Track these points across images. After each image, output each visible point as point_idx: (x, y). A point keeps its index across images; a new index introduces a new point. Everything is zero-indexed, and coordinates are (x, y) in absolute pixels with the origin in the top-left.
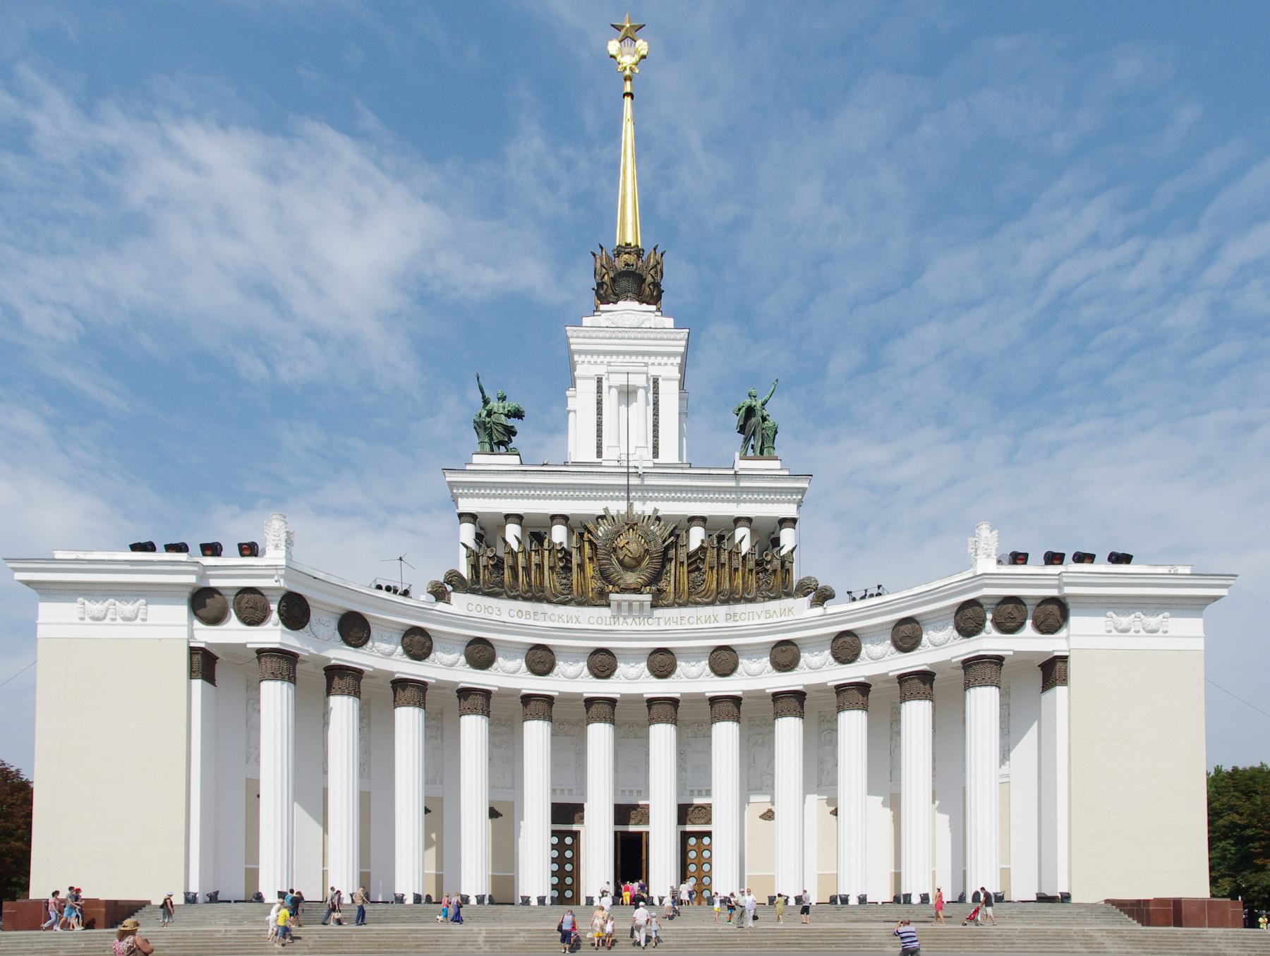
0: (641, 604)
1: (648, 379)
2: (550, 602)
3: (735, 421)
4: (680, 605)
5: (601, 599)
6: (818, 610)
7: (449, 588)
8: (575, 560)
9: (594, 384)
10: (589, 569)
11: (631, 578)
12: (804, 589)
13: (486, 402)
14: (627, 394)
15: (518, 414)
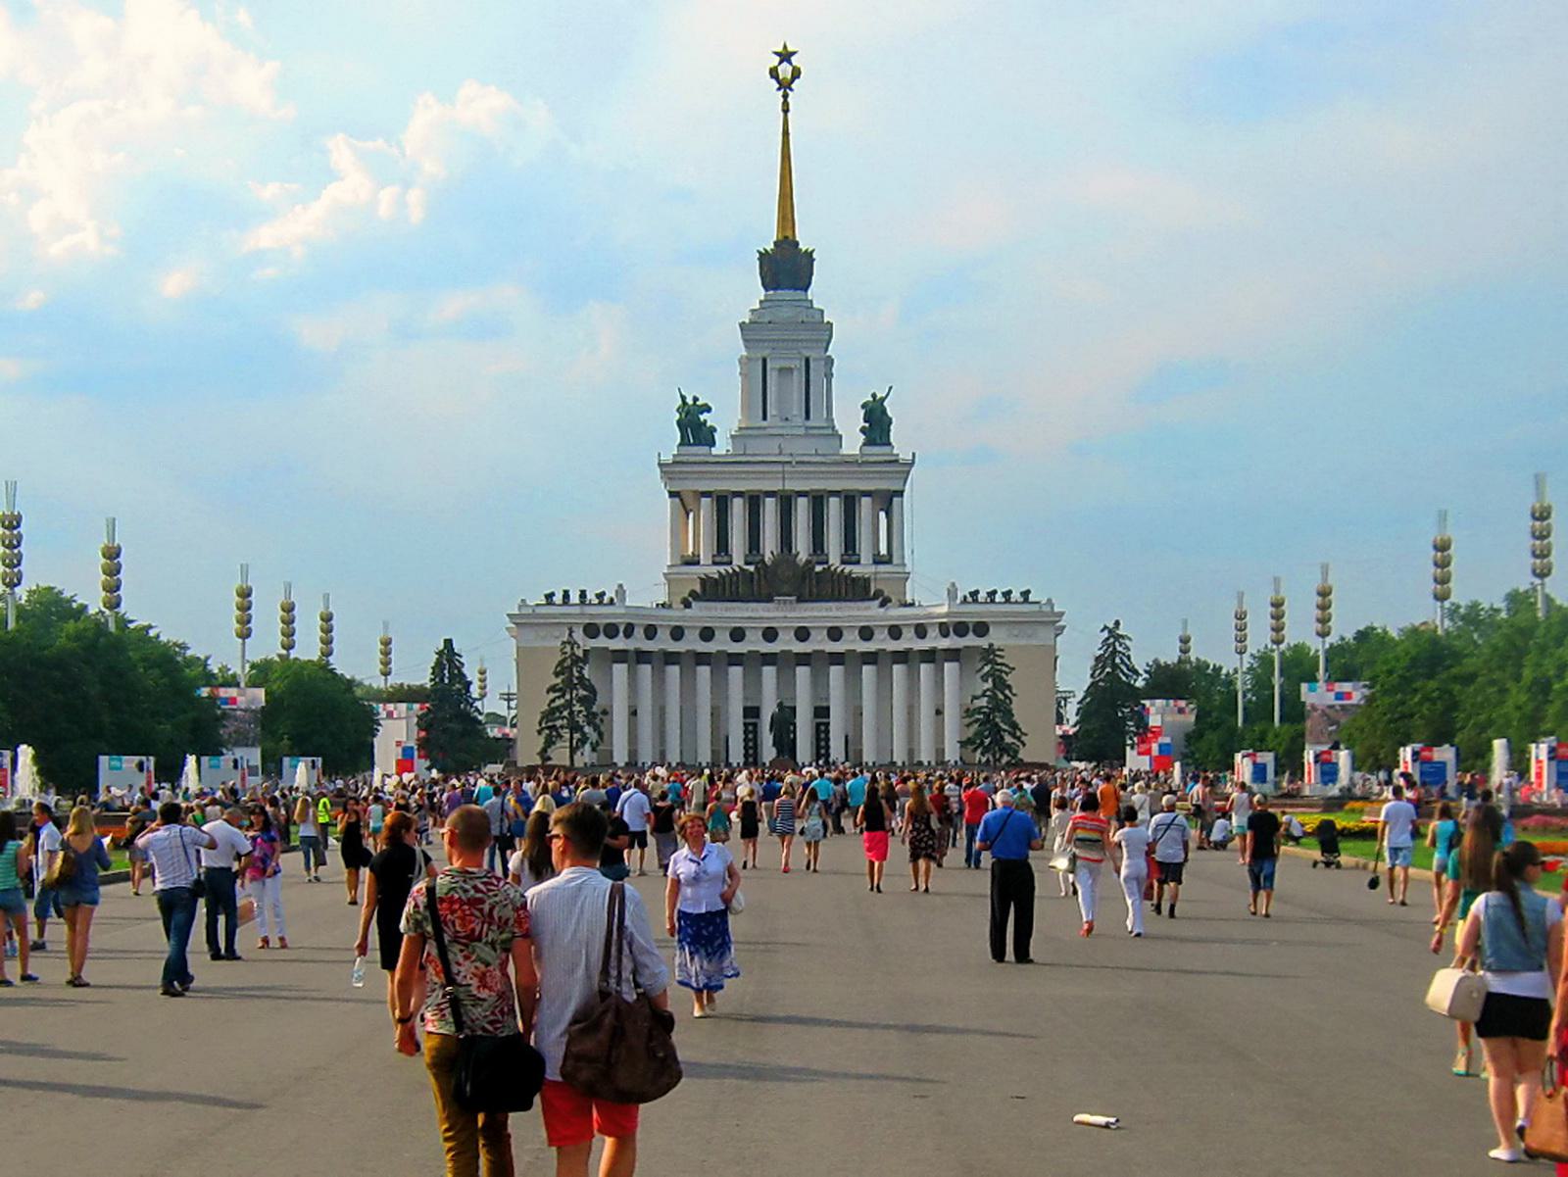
0: (791, 602)
1: (801, 360)
2: (742, 601)
3: (862, 412)
4: (812, 601)
5: (770, 600)
6: (882, 610)
7: (690, 599)
8: (756, 576)
9: (760, 363)
10: (763, 582)
11: (785, 589)
12: (875, 598)
13: (683, 398)
14: (785, 371)
15: (709, 410)
